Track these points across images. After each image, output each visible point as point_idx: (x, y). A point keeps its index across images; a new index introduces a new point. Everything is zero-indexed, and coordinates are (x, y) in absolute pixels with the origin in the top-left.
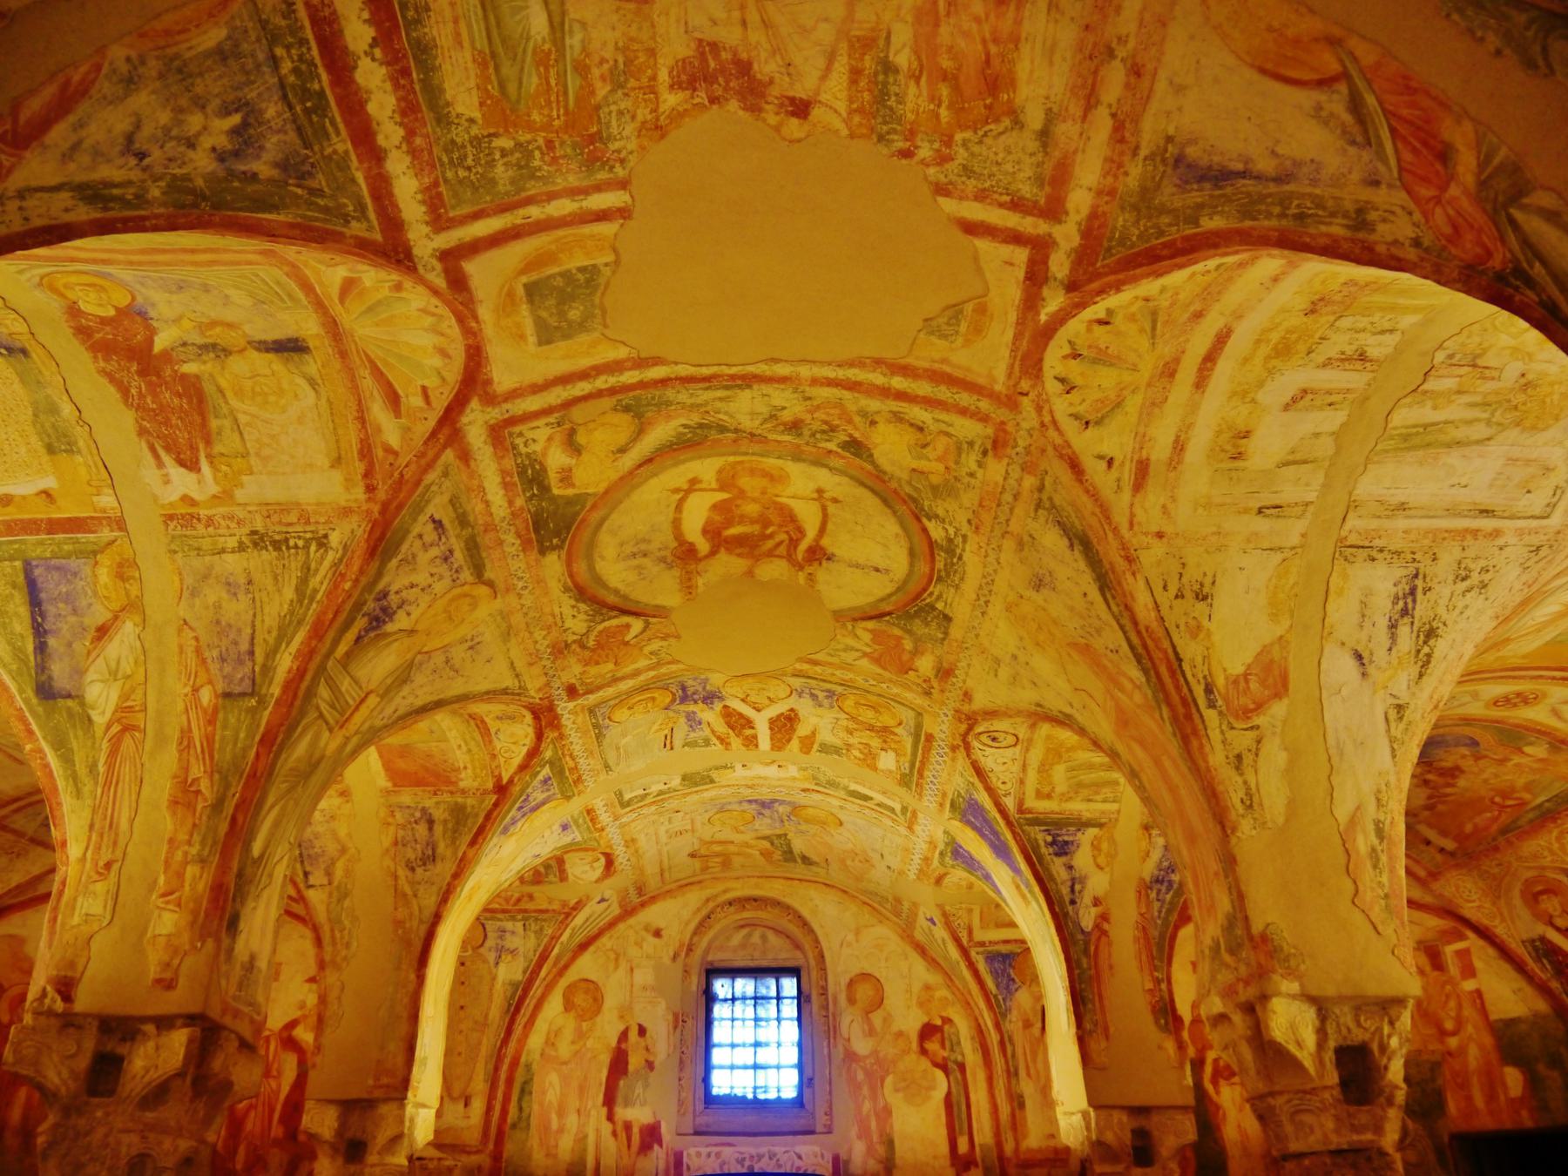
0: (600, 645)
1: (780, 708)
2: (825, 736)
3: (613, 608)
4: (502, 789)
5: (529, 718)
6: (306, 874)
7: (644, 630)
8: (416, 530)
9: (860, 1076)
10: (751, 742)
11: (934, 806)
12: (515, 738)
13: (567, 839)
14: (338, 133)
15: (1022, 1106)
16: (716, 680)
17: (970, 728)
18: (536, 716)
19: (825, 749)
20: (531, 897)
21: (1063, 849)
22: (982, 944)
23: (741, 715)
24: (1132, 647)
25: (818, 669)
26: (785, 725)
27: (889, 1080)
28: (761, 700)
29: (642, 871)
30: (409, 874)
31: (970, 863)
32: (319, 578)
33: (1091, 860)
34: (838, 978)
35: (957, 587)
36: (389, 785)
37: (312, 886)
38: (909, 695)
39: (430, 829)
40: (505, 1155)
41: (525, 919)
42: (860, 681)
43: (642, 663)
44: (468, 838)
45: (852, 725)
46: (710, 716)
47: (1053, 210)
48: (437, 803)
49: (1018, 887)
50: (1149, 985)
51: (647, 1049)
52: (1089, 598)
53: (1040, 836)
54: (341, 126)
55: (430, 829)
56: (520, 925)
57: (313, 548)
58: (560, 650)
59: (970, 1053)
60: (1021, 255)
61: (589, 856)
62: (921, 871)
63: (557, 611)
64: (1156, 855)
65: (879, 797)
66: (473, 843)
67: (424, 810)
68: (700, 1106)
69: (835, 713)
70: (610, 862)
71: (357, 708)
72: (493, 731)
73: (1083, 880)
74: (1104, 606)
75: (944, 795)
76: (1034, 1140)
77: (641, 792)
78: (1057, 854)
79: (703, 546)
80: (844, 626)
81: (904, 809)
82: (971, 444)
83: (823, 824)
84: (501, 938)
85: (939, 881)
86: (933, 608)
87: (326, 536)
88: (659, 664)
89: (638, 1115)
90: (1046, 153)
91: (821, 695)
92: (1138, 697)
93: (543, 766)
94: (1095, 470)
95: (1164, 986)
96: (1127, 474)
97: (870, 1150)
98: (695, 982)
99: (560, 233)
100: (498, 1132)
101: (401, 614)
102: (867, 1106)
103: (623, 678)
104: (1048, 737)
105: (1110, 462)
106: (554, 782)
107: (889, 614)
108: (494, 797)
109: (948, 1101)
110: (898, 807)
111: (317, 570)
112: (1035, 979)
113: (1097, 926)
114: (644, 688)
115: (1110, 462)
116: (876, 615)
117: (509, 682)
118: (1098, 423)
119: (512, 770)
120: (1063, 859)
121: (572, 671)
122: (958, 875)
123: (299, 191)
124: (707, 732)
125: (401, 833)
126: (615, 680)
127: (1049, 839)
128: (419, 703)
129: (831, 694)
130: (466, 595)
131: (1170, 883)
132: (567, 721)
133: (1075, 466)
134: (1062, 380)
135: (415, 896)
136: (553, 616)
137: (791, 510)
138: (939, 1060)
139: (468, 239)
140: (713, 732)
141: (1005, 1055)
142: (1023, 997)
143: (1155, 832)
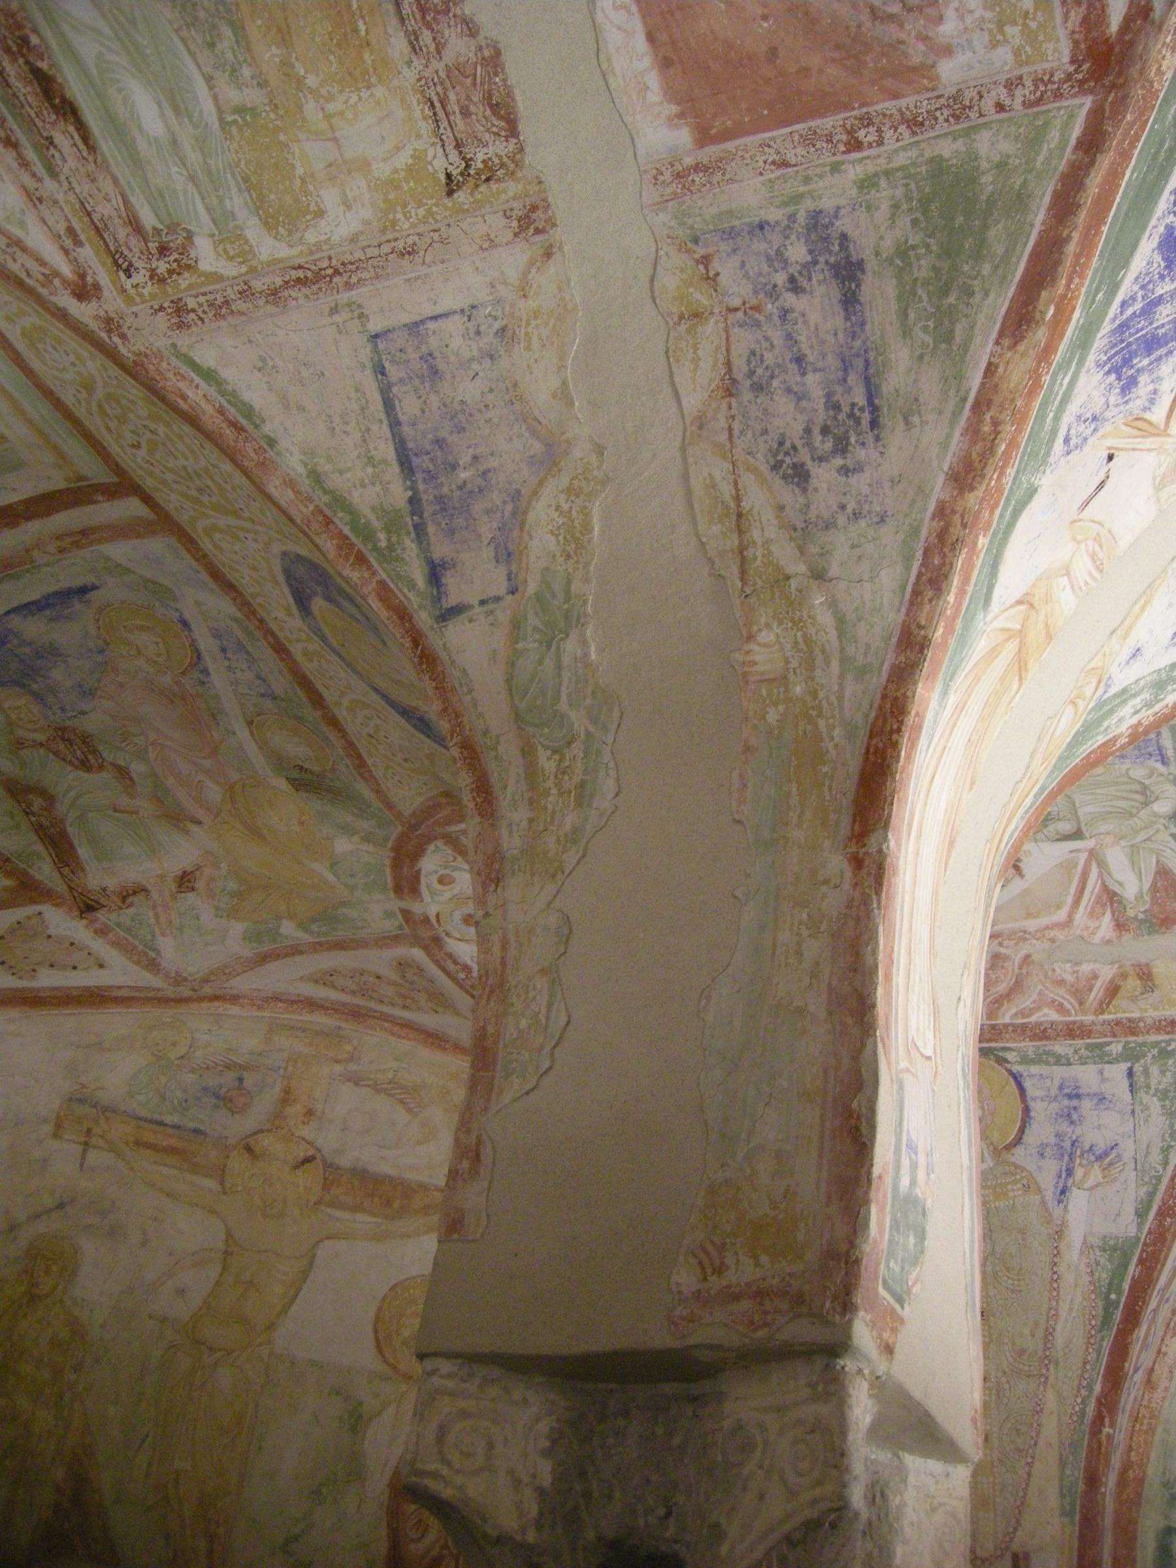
6: (435, 573)
20: (1146, 975)
30: (788, 495)
36: (684, 136)
37: (458, 610)
39: (850, 301)
41: (1132, 1055)
55: (850, 301)
84: (1068, 1116)
125: (744, 340)
135: (819, 575)
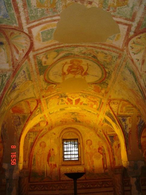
0: (48, 89)
1: (77, 98)
2: (85, 102)
3: (51, 83)
4: (31, 113)
5: (36, 101)
7: (56, 86)
8: (21, 72)
9: (89, 156)
10: (72, 103)
11: (102, 114)
12: (33, 105)
13: (41, 120)
14: (13, 9)
15: (115, 160)
16: (67, 94)
17: (110, 101)
18: (37, 101)
19: (84, 104)
20: (34, 129)
21: (124, 120)
22: (109, 135)
23: (70, 99)
24: (140, 90)
25: (84, 92)
26: (78, 101)
27: (93, 156)
28: (74, 97)
29: (52, 124)
31: (108, 122)
32: (5, 81)
33: (129, 122)
34: (85, 139)
35: (110, 79)
36: (13, 113)
38: (100, 96)
40: (32, 169)
42: (91, 94)
43: (55, 92)
44: (26, 121)
45: (89, 101)
46: (65, 100)
47: (133, 20)
48: (21, 115)
49: (116, 126)
50: (137, 141)
51: (54, 152)
52: (133, 82)
53: (120, 118)
54: (13, 8)
56: (32, 133)
57: (4, 76)
58: (42, 90)
59: (106, 152)
60: (126, 27)
61: (44, 122)
62: (99, 123)
63: (42, 84)
64: (139, 121)
65: (92, 112)
66: (27, 122)
67: (18, 117)
68: (63, 161)
69: (87, 99)
70: (47, 123)
71: (10, 102)
72: (30, 103)
73: (127, 125)
74: (136, 83)
75: (104, 112)
76: (117, 165)
77: (53, 112)
78: (123, 121)
79: (67, 73)
80: (89, 85)
81: (97, 114)
82: (115, 57)
83: (83, 116)
85: (102, 125)
86: (105, 82)
87: (6, 74)
88: (58, 92)
89: (53, 163)
90: (132, 11)
91: (84, 96)
92: (141, 98)
93: (38, 109)
94: (135, 61)
95: (140, 142)
96: (141, 62)
97: (90, 167)
98: (61, 141)
99: (48, 23)
100: (30, 165)
101: (18, 86)
102: (90, 160)
103: (52, 94)
104: (123, 103)
105: (138, 60)
106: (40, 111)
107: (98, 83)
108: (30, 114)
109: (103, 159)
110: (96, 113)
111: (4, 80)
112: (118, 140)
113: (129, 132)
114: (55, 96)
115: (138, 60)
116: (95, 83)
117: (33, 96)
118: (137, 54)
119: (33, 110)
120: (124, 122)
121: (44, 93)
122: (106, 124)
123: (6, 20)
124: (65, 102)
125: (15, 120)
126: (50, 95)
127: (122, 119)
128: (20, 100)
129: (86, 96)
130: (27, 83)
131: (141, 125)
132: (42, 101)
133: (132, 60)
134: (131, 47)
136: (41, 85)
137: (82, 67)
138: (101, 153)
139: (32, 25)
140: (66, 102)
141: (112, 152)
142: (115, 143)
143: (139, 117)
